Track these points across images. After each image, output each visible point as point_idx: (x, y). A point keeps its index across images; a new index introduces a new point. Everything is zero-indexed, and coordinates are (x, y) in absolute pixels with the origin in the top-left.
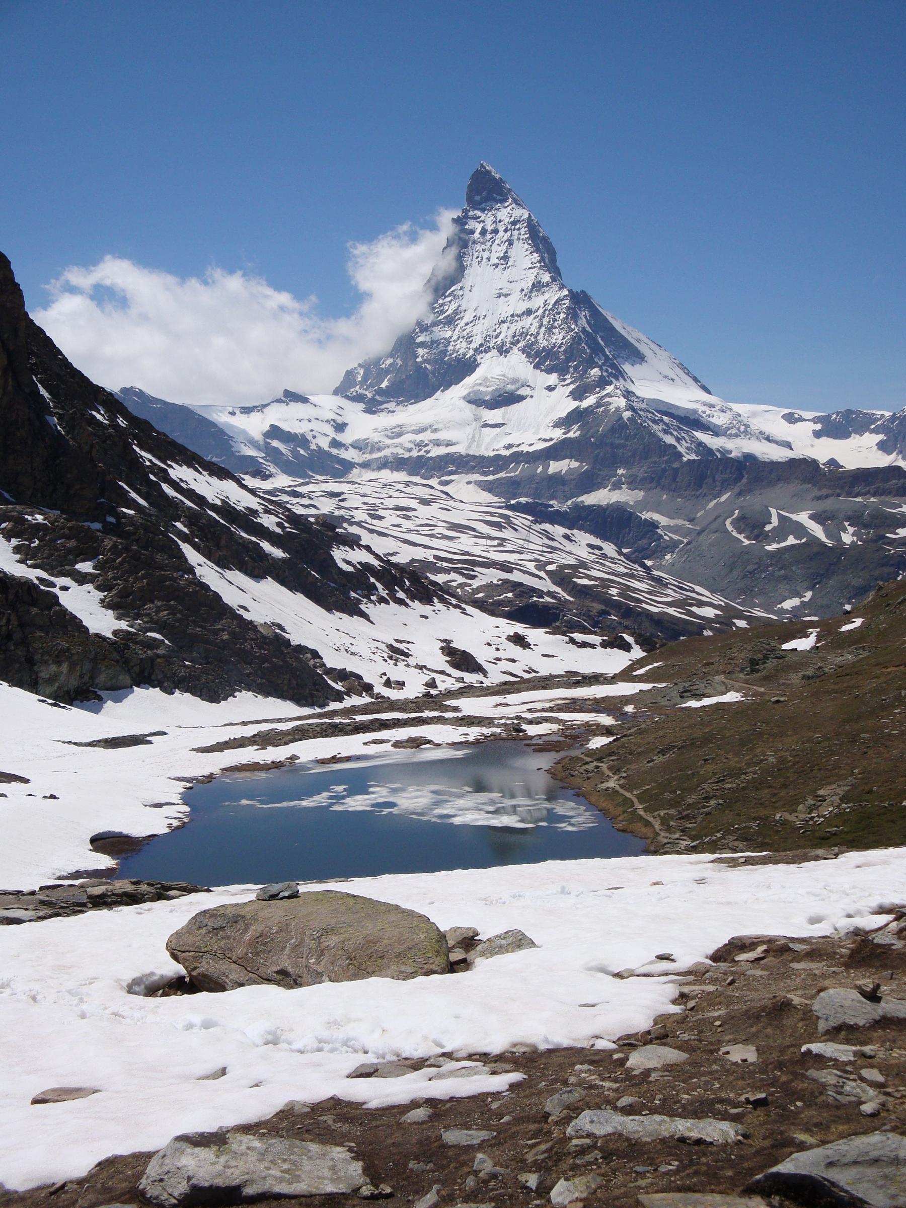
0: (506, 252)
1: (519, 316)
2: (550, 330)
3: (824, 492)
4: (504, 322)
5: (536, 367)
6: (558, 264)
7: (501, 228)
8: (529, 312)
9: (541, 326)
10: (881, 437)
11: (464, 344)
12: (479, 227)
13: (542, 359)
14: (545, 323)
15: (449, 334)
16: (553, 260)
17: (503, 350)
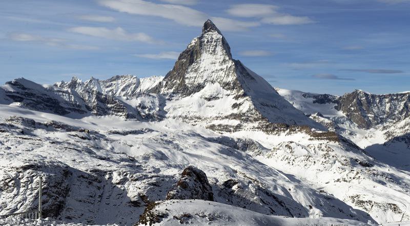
0: (215, 49)
1: (219, 71)
2: (228, 76)
3: (312, 138)
4: (214, 72)
5: (223, 88)
6: (231, 52)
7: (213, 41)
8: (222, 70)
9: (225, 74)
10: (336, 105)
11: (201, 79)
12: (206, 40)
13: (226, 85)
14: (227, 73)
15: (195, 75)
16: (230, 51)
17: (213, 82)
